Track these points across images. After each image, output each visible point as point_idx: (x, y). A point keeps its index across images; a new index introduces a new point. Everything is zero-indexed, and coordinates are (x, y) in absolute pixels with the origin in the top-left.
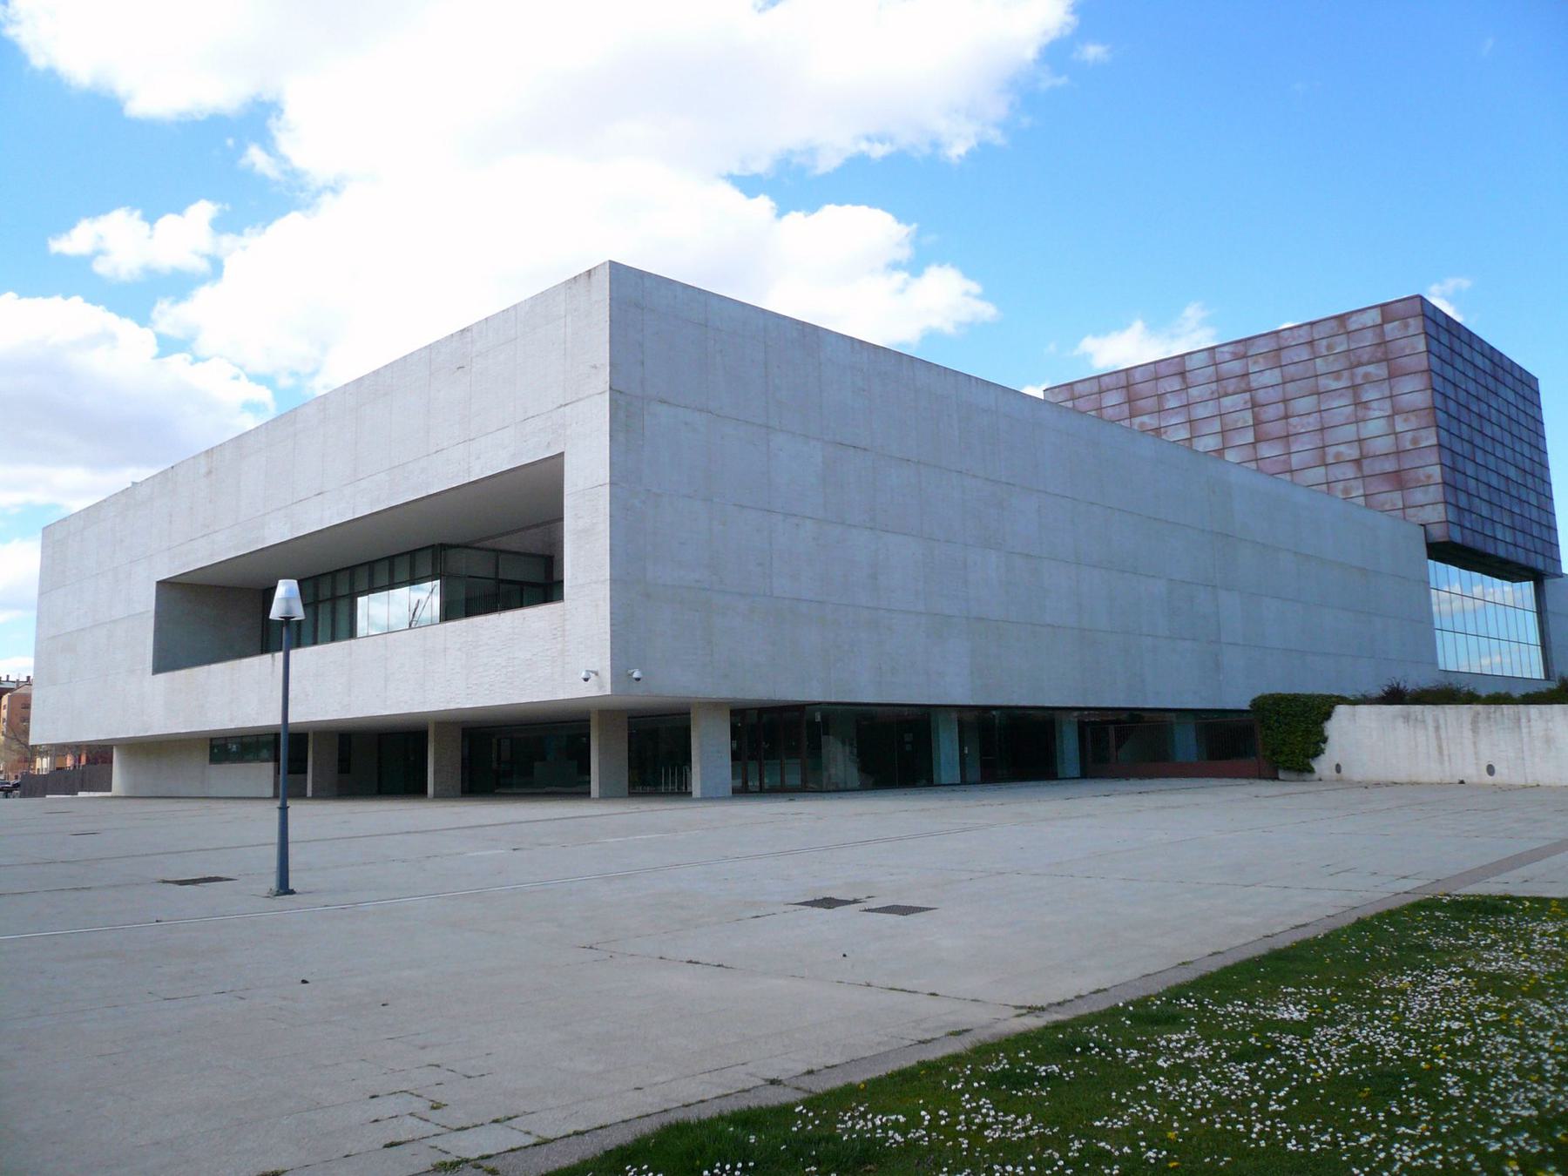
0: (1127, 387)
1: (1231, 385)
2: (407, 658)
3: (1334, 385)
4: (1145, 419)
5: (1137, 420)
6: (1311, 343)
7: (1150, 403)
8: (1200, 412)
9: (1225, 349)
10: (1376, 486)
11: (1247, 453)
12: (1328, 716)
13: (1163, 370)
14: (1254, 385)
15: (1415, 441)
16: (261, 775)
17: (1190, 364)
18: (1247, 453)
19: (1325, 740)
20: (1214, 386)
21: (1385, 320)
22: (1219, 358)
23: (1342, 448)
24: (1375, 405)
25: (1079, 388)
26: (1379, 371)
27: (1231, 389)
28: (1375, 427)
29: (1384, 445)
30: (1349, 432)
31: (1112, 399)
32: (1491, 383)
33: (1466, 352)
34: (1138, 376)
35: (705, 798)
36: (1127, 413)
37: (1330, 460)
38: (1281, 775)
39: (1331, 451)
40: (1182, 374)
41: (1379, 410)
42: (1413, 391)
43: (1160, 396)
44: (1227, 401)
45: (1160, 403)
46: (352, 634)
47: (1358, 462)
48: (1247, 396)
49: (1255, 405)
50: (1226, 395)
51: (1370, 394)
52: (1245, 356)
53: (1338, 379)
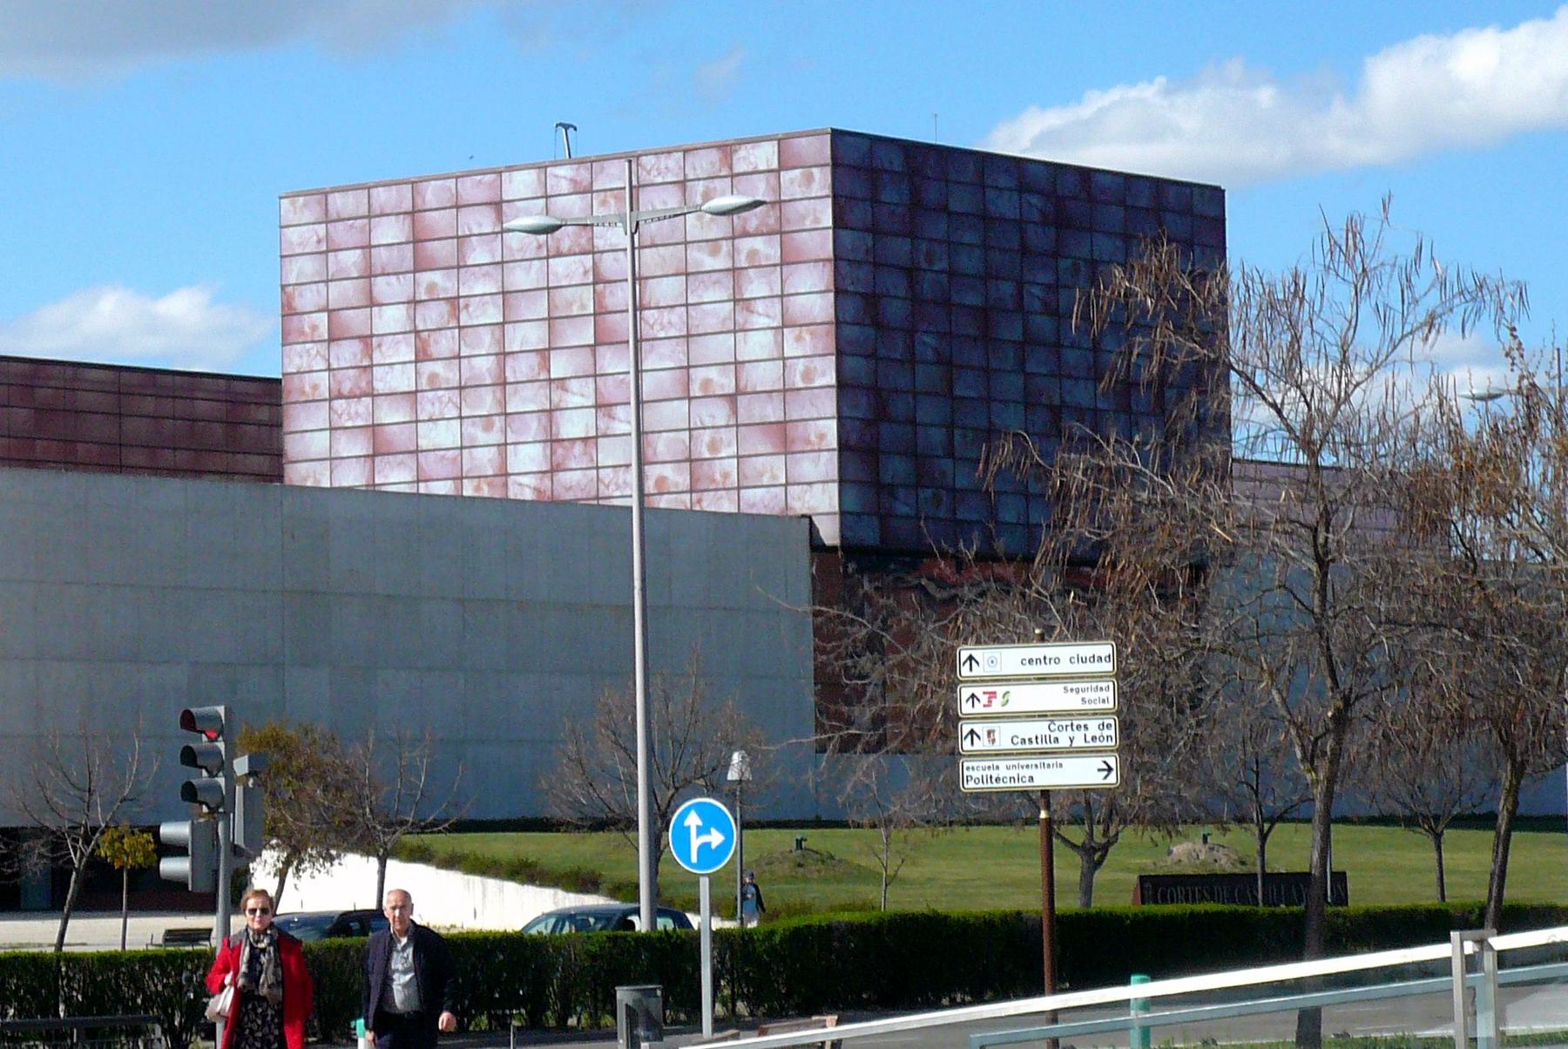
1: (566, 238)
3: (710, 263)
4: (436, 277)
6: (683, 184)
8: (521, 278)
10: (757, 443)
15: (807, 375)
21: (783, 166)
23: (713, 373)
24: (760, 306)
26: (768, 249)
28: (757, 344)
29: (764, 376)
30: (720, 347)
32: (1040, 238)
33: (961, 201)
37: (696, 390)
39: (698, 375)
41: (765, 315)
42: (813, 293)
44: (558, 264)
47: (732, 398)
48: (588, 260)
50: (559, 255)
51: (756, 286)
52: (589, 190)
53: (715, 252)
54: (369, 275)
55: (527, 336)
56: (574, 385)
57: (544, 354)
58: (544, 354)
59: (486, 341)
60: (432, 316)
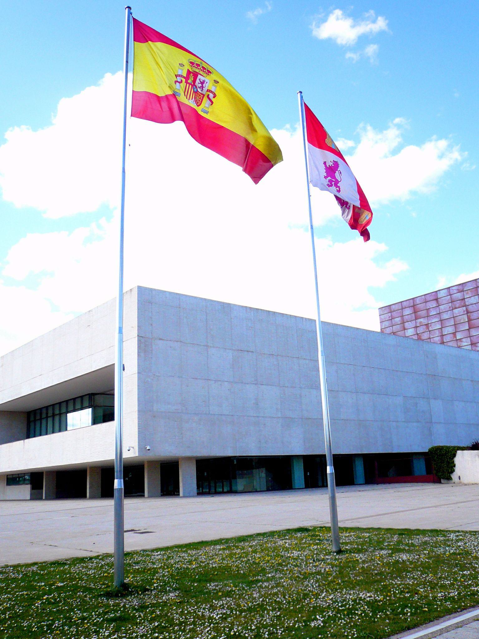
0: (414, 306)
1: (457, 304)
2: (79, 442)
4: (422, 320)
5: (419, 321)
7: (423, 313)
8: (445, 316)
9: (453, 288)
11: (466, 334)
12: (455, 455)
13: (428, 298)
14: (467, 303)
16: (25, 490)
17: (441, 295)
18: (466, 334)
19: (455, 466)
20: (450, 304)
22: (452, 292)
25: (393, 307)
27: (457, 306)
31: (407, 312)
34: (418, 301)
35: (184, 497)
36: (414, 318)
38: (442, 481)
40: (437, 300)
43: (428, 310)
44: (456, 311)
45: (428, 313)
46: (66, 430)
48: (464, 308)
49: (468, 312)
50: (456, 308)
52: (463, 291)
54: (403, 323)
55: (451, 330)
56: (464, 340)
57: (454, 334)
58: (454, 334)
59: (437, 333)
60: (420, 330)
